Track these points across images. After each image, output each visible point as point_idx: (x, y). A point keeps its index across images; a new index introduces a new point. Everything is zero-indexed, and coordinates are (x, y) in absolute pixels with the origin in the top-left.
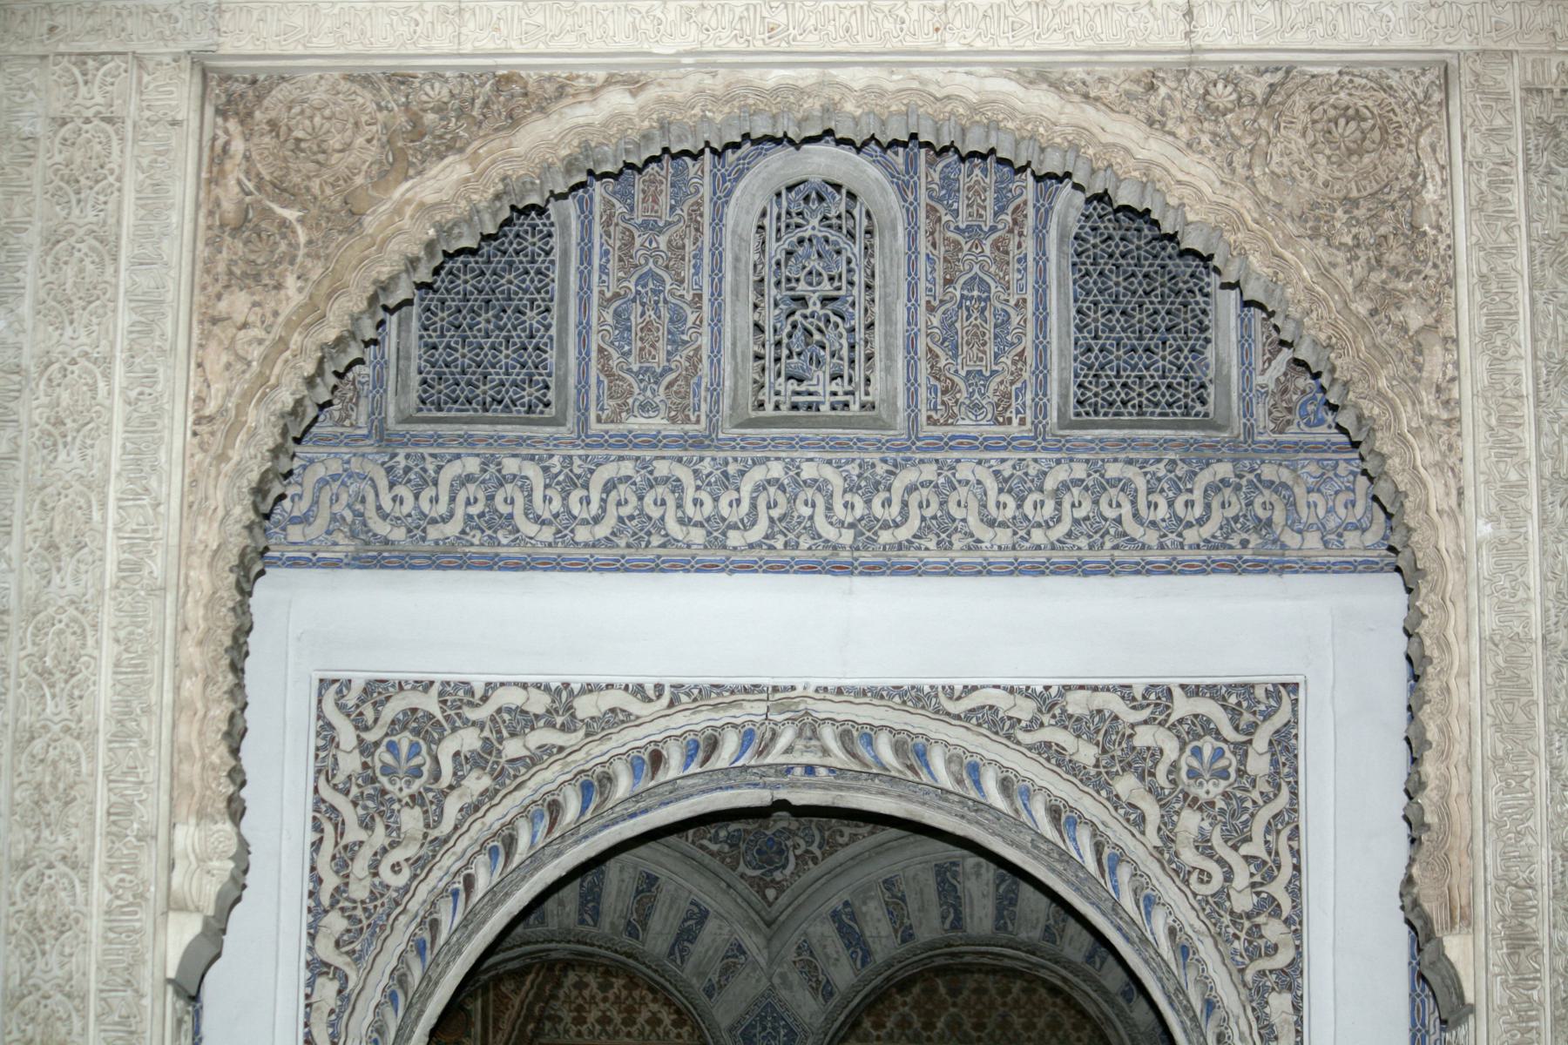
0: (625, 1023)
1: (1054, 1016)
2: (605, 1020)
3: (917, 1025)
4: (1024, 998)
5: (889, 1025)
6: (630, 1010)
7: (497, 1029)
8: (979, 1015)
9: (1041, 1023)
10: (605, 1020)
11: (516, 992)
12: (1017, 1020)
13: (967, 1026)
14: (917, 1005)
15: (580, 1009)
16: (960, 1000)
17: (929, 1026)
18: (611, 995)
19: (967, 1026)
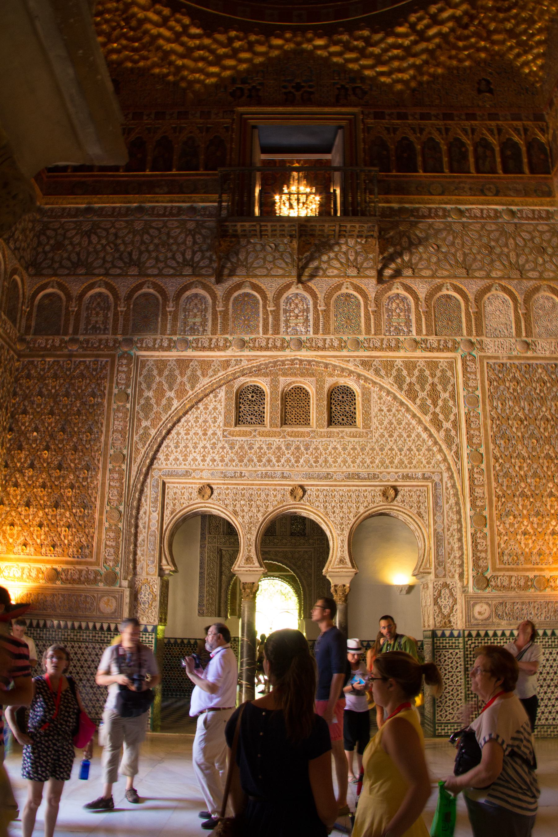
0: (184, 460)
1: (344, 458)
2: (176, 459)
3: (293, 461)
4: (333, 451)
5: (283, 461)
6: (185, 455)
7: (135, 462)
8: (317, 457)
9: (339, 461)
10: (176, 459)
11: (143, 447)
12: (330, 460)
13: (312, 462)
14: (293, 454)
15: (167, 455)
16: (309, 452)
17: (297, 461)
18: (179, 450)
19: (312, 462)
